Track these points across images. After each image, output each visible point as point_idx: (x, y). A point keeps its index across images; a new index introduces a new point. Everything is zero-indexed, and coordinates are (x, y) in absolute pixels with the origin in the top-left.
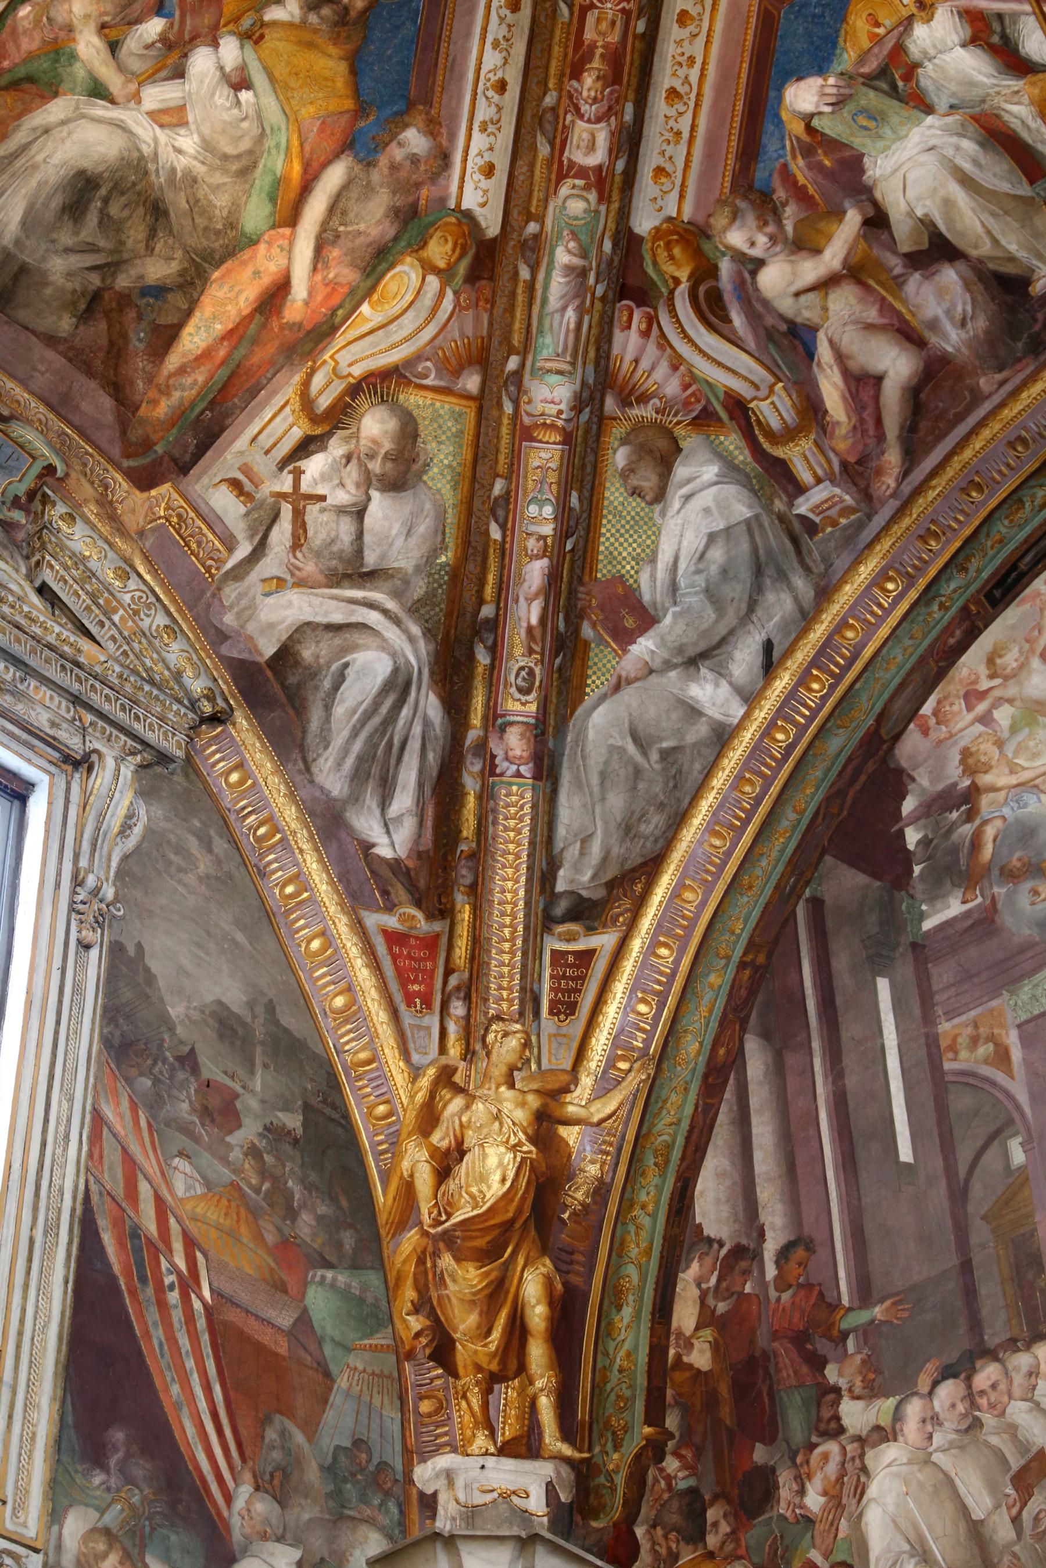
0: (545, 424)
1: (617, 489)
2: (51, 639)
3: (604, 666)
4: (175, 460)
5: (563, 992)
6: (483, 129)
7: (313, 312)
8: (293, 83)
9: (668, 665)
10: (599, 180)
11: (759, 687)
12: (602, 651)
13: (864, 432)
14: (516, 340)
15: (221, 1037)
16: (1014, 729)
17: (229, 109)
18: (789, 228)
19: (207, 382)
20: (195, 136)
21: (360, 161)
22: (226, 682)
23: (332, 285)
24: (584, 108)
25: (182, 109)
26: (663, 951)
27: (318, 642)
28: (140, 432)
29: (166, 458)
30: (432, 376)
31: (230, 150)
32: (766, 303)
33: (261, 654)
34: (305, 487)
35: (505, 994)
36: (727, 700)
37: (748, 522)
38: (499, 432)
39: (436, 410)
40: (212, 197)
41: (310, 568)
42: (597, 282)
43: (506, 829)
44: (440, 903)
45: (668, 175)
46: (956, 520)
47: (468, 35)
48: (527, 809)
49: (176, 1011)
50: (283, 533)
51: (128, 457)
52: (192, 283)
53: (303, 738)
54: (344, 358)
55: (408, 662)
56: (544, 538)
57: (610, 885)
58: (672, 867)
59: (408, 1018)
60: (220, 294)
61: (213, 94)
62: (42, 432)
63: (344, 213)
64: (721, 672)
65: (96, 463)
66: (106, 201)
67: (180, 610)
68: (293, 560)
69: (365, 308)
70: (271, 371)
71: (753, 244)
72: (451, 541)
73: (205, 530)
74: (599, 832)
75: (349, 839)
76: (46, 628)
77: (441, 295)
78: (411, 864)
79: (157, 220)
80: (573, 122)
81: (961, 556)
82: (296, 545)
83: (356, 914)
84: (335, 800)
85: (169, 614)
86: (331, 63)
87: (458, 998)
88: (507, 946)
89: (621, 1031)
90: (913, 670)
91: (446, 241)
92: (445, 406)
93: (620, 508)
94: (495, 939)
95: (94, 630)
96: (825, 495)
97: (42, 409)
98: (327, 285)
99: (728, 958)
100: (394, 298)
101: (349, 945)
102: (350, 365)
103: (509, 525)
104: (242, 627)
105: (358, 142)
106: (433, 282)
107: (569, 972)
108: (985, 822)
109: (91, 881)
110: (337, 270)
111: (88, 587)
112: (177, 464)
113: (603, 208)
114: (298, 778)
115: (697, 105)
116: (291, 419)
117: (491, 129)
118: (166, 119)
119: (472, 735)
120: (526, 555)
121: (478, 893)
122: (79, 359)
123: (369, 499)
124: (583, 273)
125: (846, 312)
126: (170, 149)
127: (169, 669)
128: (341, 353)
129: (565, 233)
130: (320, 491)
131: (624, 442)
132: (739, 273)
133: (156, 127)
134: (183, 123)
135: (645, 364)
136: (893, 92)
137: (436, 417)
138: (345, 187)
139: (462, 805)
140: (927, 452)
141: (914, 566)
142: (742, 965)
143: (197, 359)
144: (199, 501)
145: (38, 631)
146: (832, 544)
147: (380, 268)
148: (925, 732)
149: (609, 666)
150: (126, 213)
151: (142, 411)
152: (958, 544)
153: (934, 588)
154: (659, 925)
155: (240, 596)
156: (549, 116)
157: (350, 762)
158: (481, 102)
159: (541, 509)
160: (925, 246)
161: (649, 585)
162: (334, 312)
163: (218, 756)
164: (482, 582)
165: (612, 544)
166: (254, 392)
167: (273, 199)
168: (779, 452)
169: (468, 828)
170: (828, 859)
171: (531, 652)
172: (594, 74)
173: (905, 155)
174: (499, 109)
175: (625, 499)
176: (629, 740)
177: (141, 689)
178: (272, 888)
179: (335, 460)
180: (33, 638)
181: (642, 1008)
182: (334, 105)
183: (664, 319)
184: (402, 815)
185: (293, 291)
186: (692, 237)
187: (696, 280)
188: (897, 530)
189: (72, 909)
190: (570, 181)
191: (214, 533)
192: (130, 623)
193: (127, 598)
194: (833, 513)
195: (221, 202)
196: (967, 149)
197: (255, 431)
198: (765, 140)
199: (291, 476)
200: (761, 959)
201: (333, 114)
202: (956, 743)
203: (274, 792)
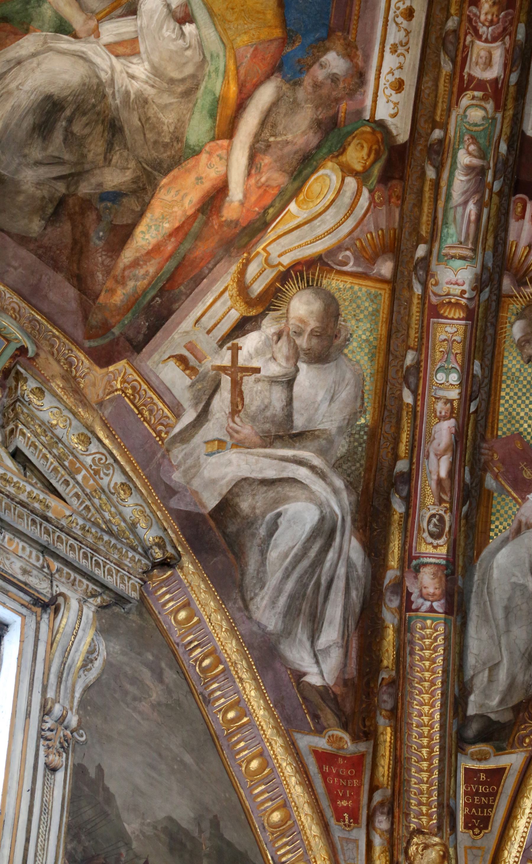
0: (450, 303)
1: (515, 358)
2: (23, 497)
3: (506, 512)
4: (130, 341)
5: (477, 807)
6: (394, 50)
7: (248, 210)
8: (229, 16)
10: (495, 91)
12: (504, 500)
14: (424, 230)
15: (172, 850)
17: (175, 40)
19: (157, 273)
20: (147, 65)
21: (288, 81)
22: (175, 532)
23: (265, 188)
24: (482, 30)
25: (135, 40)
27: (254, 495)
28: (100, 317)
29: (122, 339)
30: (351, 264)
31: (176, 75)
33: (205, 507)
34: (241, 361)
35: (424, 809)
38: (409, 311)
39: (355, 293)
40: (161, 115)
41: (247, 430)
42: (495, 178)
43: (422, 659)
44: (365, 726)
48: (440, 641)
49: (132, 826)
50: (223, 401)
51: (89, 338)
52: (144, 189)
53: (242, 580)
54: (275, 250)
55: (333, 511)
56: (451, 401)
57: (517, 709)
59: (337, 831)
60: (168, 198)
61: (161, 27)
62: (15, 319)
63: (274, 126)
65: (62, 343)
66: (70, 121)
67: (134, 470)
68: (232, 424)
69: (293, 207)
70: (212, 263)
72: (369, 406)
73: (156, 400)
74: (505, 661)
75: (283, 669)
76: (19, 488)
77: (358, 194)
78: (338, 690)
79: (113, 136)
80: (472, 42)
82: (235, 411)
83: (290, 736)
84: (271, 634)
85: (125, 473)
87: (382, 813)
88: (425, 765)
91: (362, 147)
92: (362, 289)
93: (517, 374)
94: (414, 758)
95: (60, 488)
97: (16, 299)
98: (259, 188)
100: (317, 197)
101: (284, 764)
102: (280, 256)
103: (420, 391)
104: (188, 483)
106: (351, 183)
107: (481, 789)
109: (57, 710)
110: (268, 175)
111: (55, 451)
112: (132, 344)
113: (499, 116)
114: (238, 615)
116: (229, 303)
117: (400, 50)
118: (121, 50)
119: (391, 575)
120: (435, 416)
121: (398, 717)
122: (47, 255)
123: (297, 370)
124: (481, 172)
126: (125, 75)
127: (125, 521)
128: (272, 246)
129: (466, 138)
130: (255, 364)
131: (520, 316)
133: (113, 57)
134: (136, 53)
138: (275, 104)
139: (383, 638)
143: (149, 253)
144: (151, 375)
145: (11, 490)
147: (305, 172)
149: (510, 512)
150: (87, 131)
151: (102, 299)
155: (187, 456)
156: (451, 38)
157: (283, 600)
158: (392, 28)
159: (447, 377)
163: (167, 597)
164: (397, 440)
165: (511, 406)
166: (198, 280)
167: (212, 115)
169: (388, 658)
171: (441, 501)
174: (408, 33)
175: (522, 366)
177: (101, 538)
178: (216, 714)
179: (267, 337)
180: (8, 496)
182: (264, 34)
184: (330, 647)
185: (230, 193)
189: (40, 736)
190: (470, 93)
191: (164, 402)
192: (92, 482)
193: (89, 460)
195: (168, 119)
197: (199, 314)
199: (230, 352)
201: (263, 42)
203: (217, 628)
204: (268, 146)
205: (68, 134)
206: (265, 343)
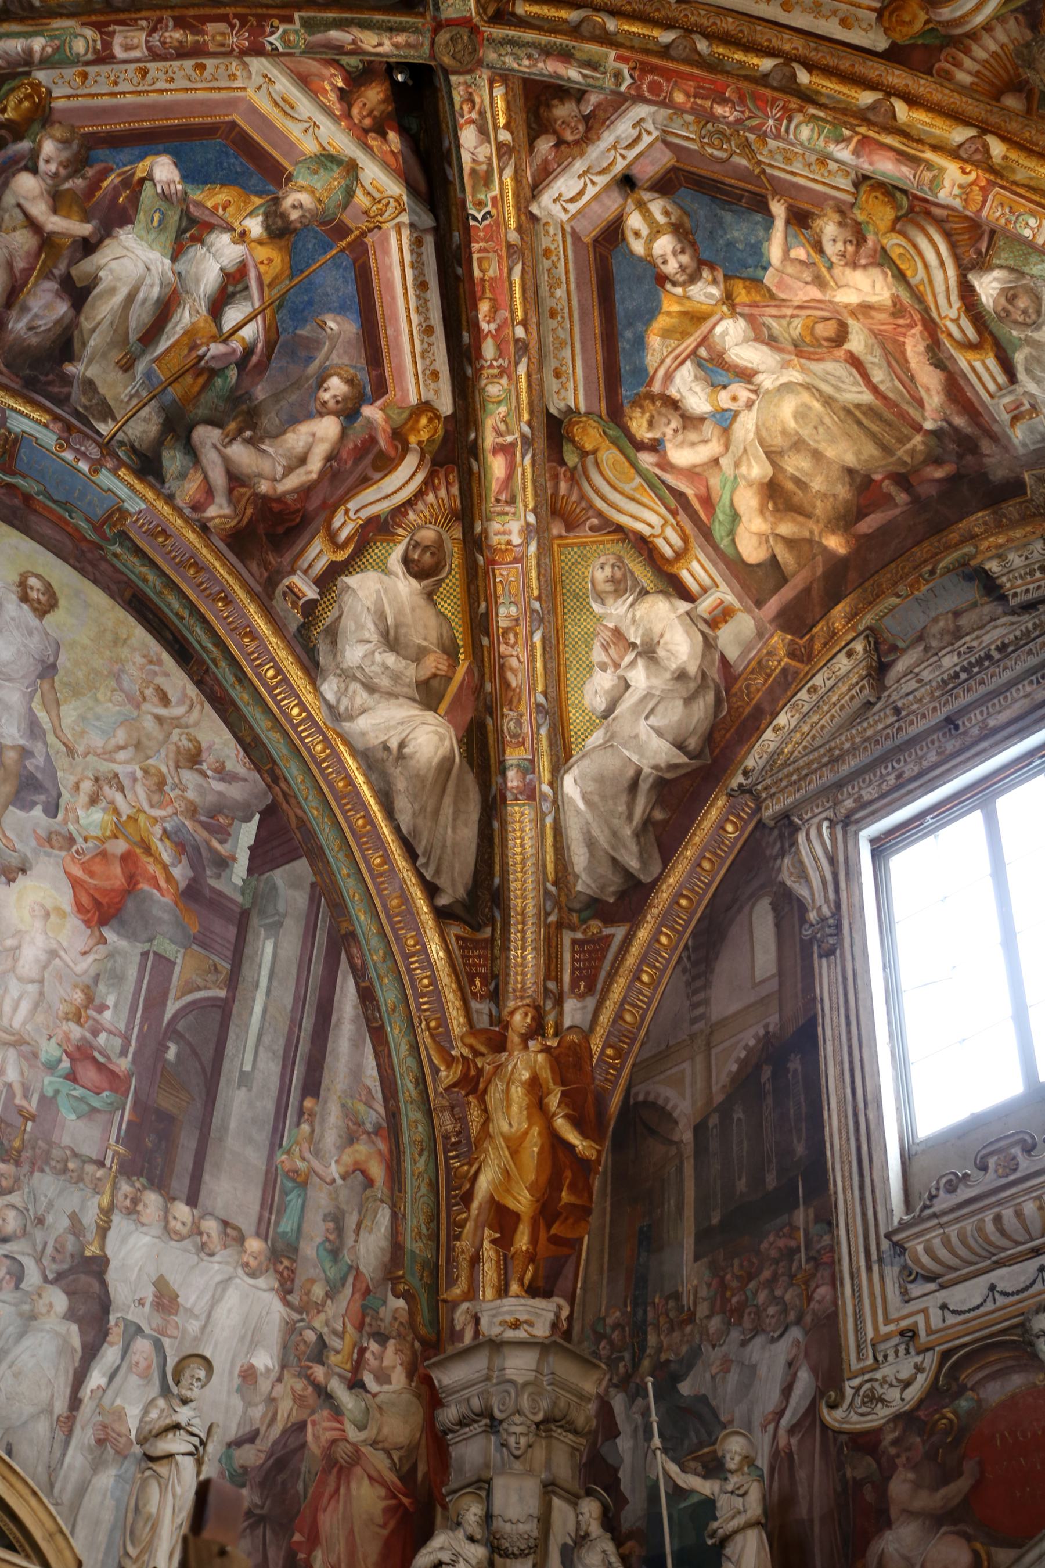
18: (67, 185)
24: (156, 36)
115: (139, 93)
132: (23, 157)
136: (181, 232)
173: (139, 252)
186: (41, 115)
190: (98, 37)
198: (127, 150)
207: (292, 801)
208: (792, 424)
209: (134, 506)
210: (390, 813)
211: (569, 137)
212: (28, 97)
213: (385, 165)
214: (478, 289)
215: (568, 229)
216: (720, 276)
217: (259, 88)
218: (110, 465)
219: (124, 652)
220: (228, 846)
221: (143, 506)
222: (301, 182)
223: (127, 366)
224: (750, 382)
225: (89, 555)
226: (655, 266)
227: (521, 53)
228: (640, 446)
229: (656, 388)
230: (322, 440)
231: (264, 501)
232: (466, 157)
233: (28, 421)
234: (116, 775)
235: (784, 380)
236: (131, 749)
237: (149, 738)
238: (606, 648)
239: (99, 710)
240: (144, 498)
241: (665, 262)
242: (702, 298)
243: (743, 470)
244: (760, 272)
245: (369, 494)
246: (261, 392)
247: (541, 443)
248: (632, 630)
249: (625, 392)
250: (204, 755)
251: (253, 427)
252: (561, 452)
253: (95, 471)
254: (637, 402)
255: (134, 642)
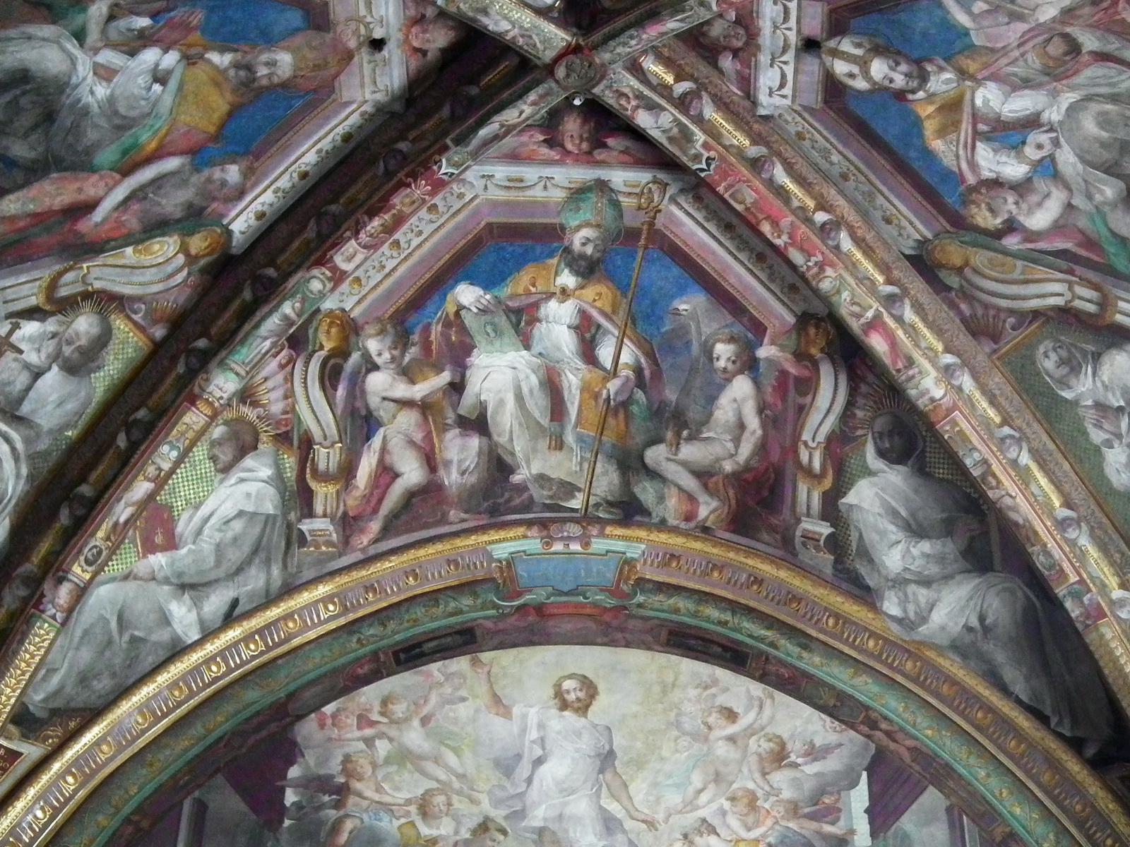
6: (275, 192)
9: (167, 581)
11: (217, 626)
13: (368, 501)
16: (388, 761)
18: (407, 359)
20: (108, 92)
23: (120, 224)
24: (362, 235)
26: (70, 779)
31: (122, 111)
32: (363, 392)
34: (13, 339)
36: (191, 625)
37: (268, 516)
43: (26, 651)
45: (360, 285)
46: (392, 589)
47: (309, 136)
48: (46, 644)
54: (96, 272)
55: (6, 490)
56: (160, 469)
57: (54, 712)
58: (105, 723)
63: (159, 188)
64: (197, 603)
66: (24, 94)
69: (129, 250)
71: (380, 355)
74: (63, 671)
77: (180, 269)
80: (350, 238)
81: (384, 614)
86: (221, 102)
89: (19, 824)
90: (325, 675)
96: (322, 526)
99: (118, 810)
105: (200, 154)
106: (181, 259)
108: (347, 816)
115: (406, 259)
116: (35, 291)
118: (102, 72)
123: (50, 368)
125: (404, 426)
130: (23, 346)
131: (226, 423)
135: (270, 384)
136: (516, 326)
137: (124, 342)
140: (398, 534)
141: (352, 603)
142: (127, 821)
146: (309, 559)
148: (322, 726)
152: (385, 604)
153: (358, 625)
154: (77, 759)
158: (286, 177)
160: (474, 417)
161: (185, 525)
162: (108, 241)
166: (23, 260)
167: (125, 153)
168: (313, 485)
170: (220, 779)
171: (108, 539)
172: (381, 221)
173: (497, 362)
176: (115, 618)
181: (39, 814)
183: (299, 365)
186: (350, 329)
187: (333, 353)
188: (355, 575)
194: (321, 540)
195: (92, 135)
196: (532, 381)
199: (10, 326)
200: (145, 824)
202: (342, 746)
204: (145, 198)
205: (16, 98)
206: (40, 335)
207: (900, 736)
208: (1105, 134)
209: (635, 551)
210: (1004, 689)
211: (740, 44)
212: (332, 323)
213: (625, 165)
214: (750, 217)
215: (799, 108)
216: (942, 63)
217: (486, 188)
218: (595, 532)
219: (676, 695)
220: (842, 823)
221: (643, 546)
222: (574, 223)
223: (559, 445)
224: (1040, 126)
225: (615, 623)
226: (887, 89)
227: (622, 39)
228: (998, 234)
229: (971, 179)
230: (744, 400)
231: (738, 479)
232: (655, 134)
233: (506, 545)
234: (704, 821)
235: (1065, 106)
236: (712, 786)
237: (726, 763)
238: (1098, 426)
239: (668, 767)
240: (639, 540)
241: (891, 81)
242: (945, 87)
243: (1098, 197)
244: (966, 40)
245: (814, 419)
246: (671, 395)
247: (917, 285)
248: (1110, 396)
249: (951, 200)
250: (789, 747)
251: (685, 425)
252: (941, 281)
253: (586, 545)
254: (965, 203)
255: (683, 679)
